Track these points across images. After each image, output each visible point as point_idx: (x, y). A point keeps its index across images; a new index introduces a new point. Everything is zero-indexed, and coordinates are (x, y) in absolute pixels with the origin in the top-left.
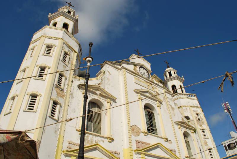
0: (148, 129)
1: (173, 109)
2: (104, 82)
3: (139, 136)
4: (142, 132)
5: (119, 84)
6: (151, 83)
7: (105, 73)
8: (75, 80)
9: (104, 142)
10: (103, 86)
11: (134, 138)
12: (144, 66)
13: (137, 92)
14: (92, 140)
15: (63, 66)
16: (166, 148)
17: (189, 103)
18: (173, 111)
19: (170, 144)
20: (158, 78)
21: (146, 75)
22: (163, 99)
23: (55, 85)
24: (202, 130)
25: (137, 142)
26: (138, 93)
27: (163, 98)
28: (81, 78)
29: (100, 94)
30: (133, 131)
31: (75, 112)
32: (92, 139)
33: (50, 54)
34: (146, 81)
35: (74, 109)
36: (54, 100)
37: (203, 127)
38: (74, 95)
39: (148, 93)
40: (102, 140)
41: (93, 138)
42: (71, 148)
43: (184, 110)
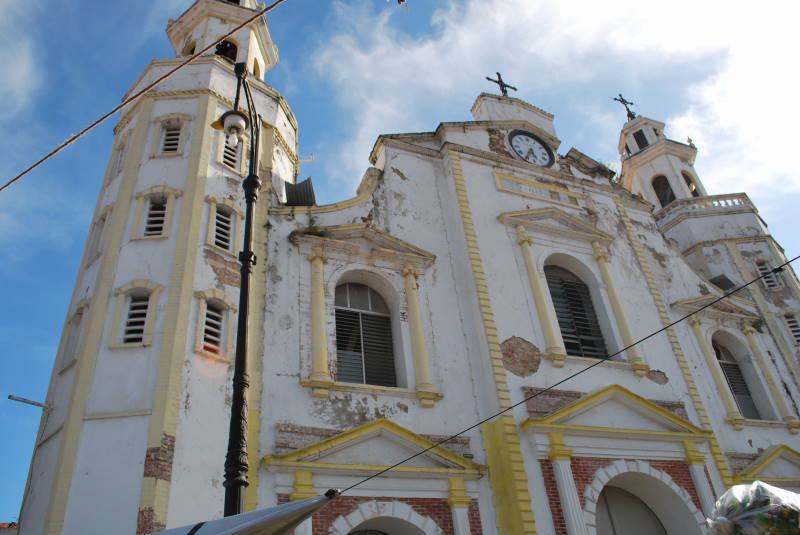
0: (565, 343)
1: (660, 261)
2: (385, 209)
7: (386, 176)
8: (277, 221)
9: (406, 409)
10: (382, 222)
11: (514, 383)
14: (363, 408)
15: (228, 179)
17: (722, 227)
18: (663, 266)
19: (660, 383)
21: (540, 157)
22: (616, 229)
24: (787, 317)
25: (531, 394)
27: (618, 226)
28: (297, 208)
30: (510, 357)
31: (289, 326)
32: (363, 405)
33: (176, 149)
35: (288, 317)
36: (209, 295)
37: (788, 306)
38: (281, 272)
40: (400, 406)
41: (366, 404)
42: (291, 445)
43: (708, 256)
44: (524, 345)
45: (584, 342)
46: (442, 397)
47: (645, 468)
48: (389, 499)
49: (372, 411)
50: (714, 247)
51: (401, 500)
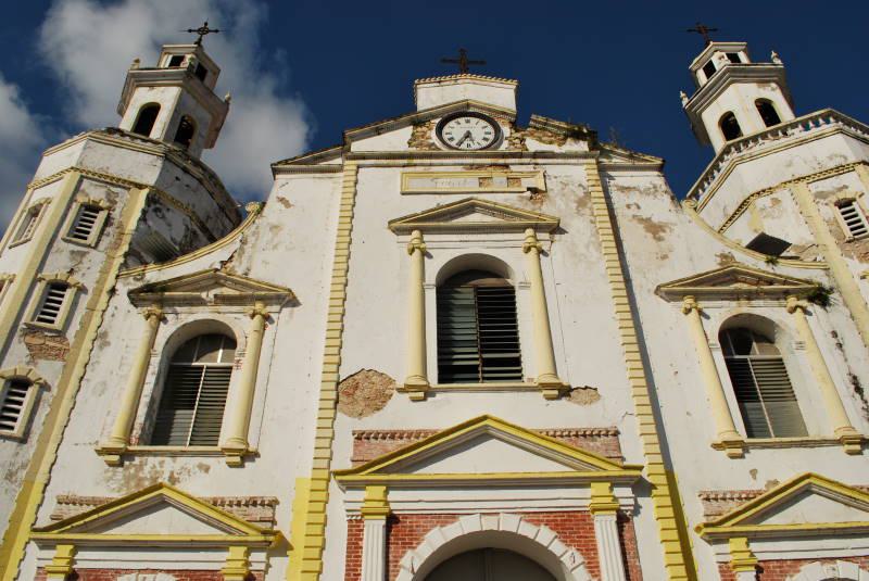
3: (378, 409)
4: (401, 390)
5: (327, 230)
6: (501, 161)
9: (207, 469)
12: (475, 106)
13: (400, 228)
14: (157, 472)
15: (73, 252)
16: (526, 432)
17: (790, 165)
18: (660, 239)
20: (557, 123)
23: (21, 326)
26: (409, 231)
29: (215, 296)
32: (158, 469)
34: (472, 165)
39: (474, 212)
40: (200, 466)
41: (161, 467)
44: (374, 379)
45: (487, 362)
46: (256, 455)
47: (509, 524)
48: (154, 571)
49: (167, 475)
50: (774, 196)
51: (168, 571)
